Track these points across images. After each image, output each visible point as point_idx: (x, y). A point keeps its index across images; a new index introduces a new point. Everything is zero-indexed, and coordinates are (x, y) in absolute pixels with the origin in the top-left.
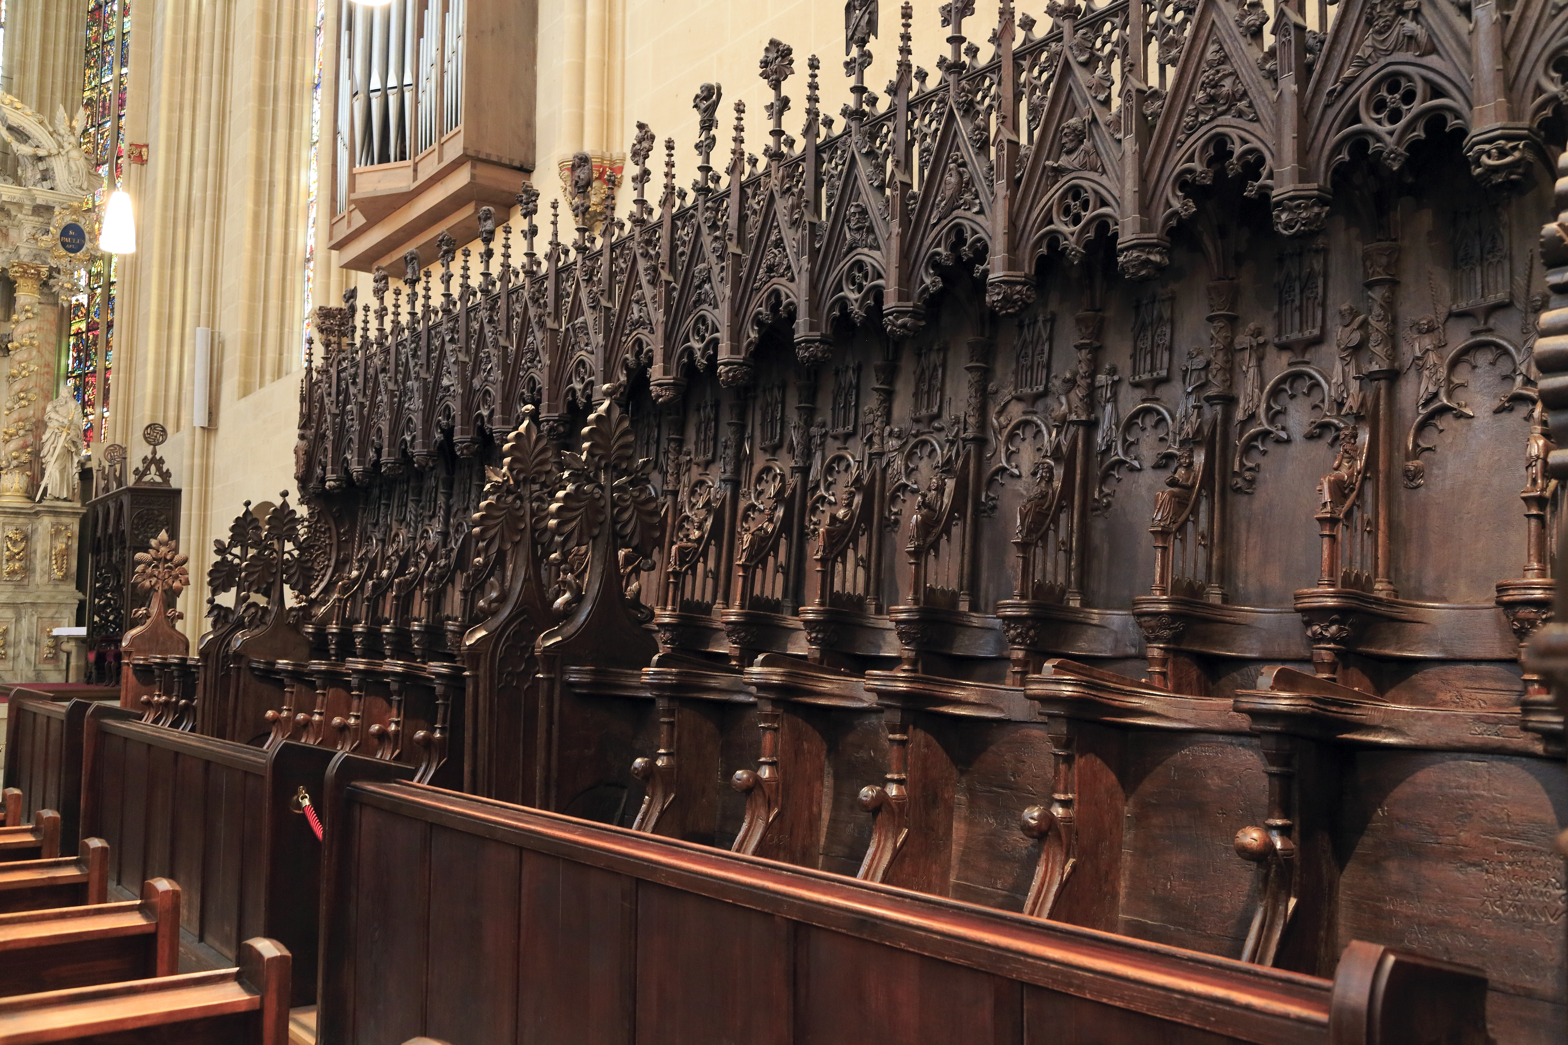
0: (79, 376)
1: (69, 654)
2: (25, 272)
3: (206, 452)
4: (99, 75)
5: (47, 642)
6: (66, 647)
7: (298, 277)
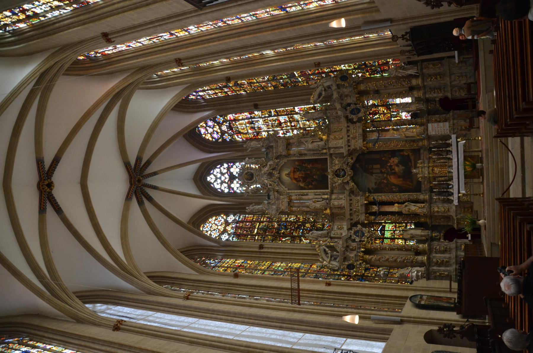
1: (464, 58)
3: (398, 21)
4: (300, 82)
5: (460, 65)
6: (461, 59)
7: (341, 3)
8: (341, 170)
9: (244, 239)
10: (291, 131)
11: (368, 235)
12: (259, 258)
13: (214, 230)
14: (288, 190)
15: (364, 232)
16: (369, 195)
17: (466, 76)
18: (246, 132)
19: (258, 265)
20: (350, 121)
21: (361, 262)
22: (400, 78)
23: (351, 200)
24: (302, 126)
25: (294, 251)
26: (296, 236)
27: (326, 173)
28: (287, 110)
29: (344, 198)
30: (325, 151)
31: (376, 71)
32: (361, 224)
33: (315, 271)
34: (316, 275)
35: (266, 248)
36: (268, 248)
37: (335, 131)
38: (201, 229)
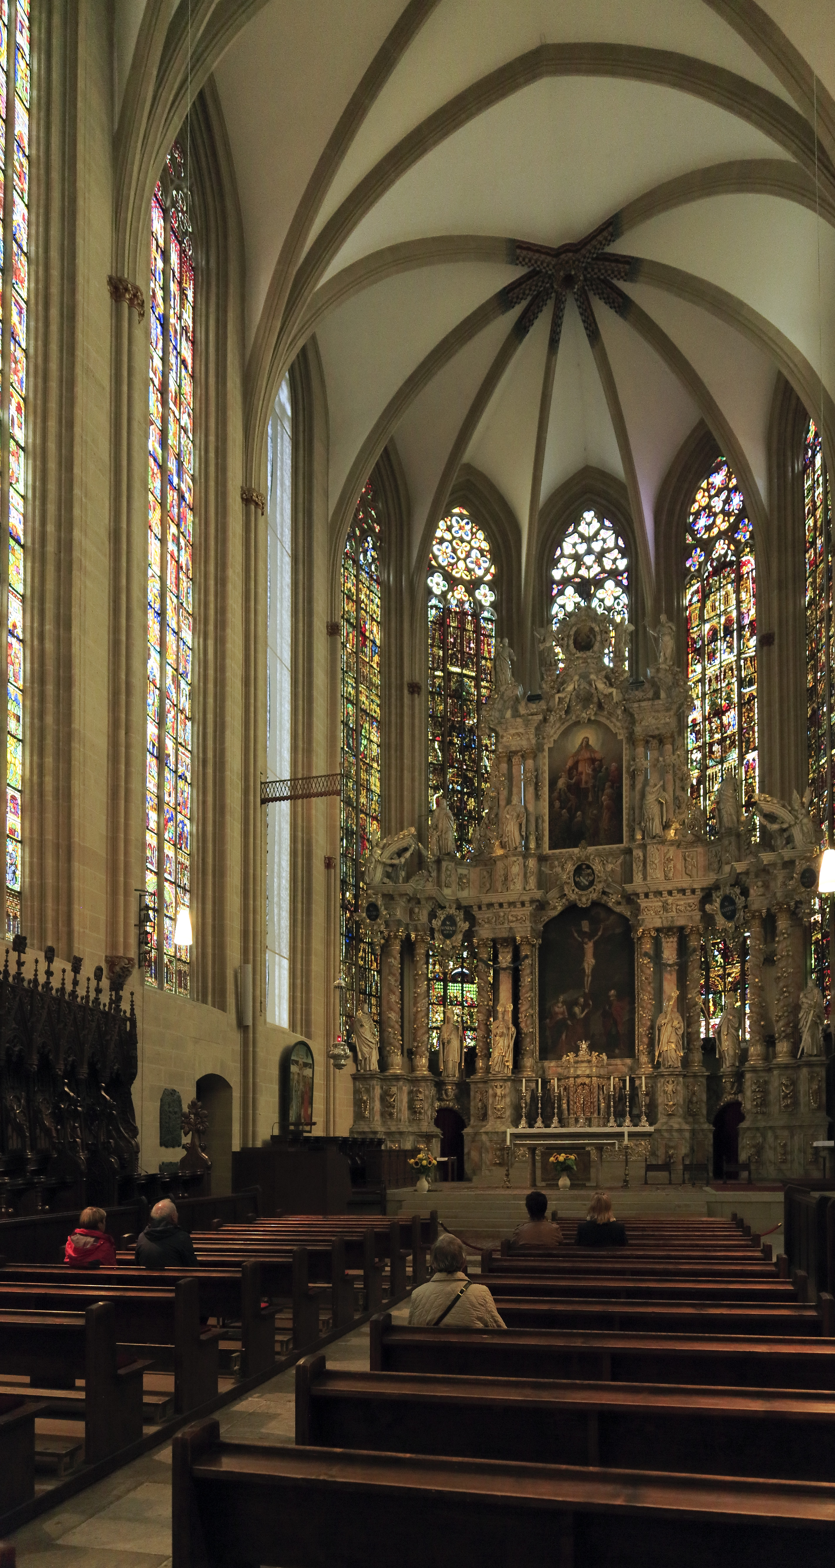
0: (819, 970)
1: (824, 1159)
2: (781, 908)
5: (810, 1151)
6: (824, 1154)
8: (591, 878)
9: (433, 639)
10: (699, 744)
11: (447, 946)
12: (386, 686)
13: (454, 551)
14: (549, 748)
15: (454, 938)
16: (534, 946)
17: (784, 1161)
18: (706, 617)
19: (370, 686)
20: (707, 896)
21: (386, 933)
22: (796, 1015)
23: (523, 904)
24: (709, 772)
25: (406, 774)
26: (445, 774)
27: (583, 842)
28: (752, 728)
29: (527, 888)
30: (639, 836)
31: (824, 957)
32: (470, 928)
33: (364, 830)
34: (353, 833)
35: (413, 701)
36: (412, 707)
37: (685, 860)
38: (456, 510)
